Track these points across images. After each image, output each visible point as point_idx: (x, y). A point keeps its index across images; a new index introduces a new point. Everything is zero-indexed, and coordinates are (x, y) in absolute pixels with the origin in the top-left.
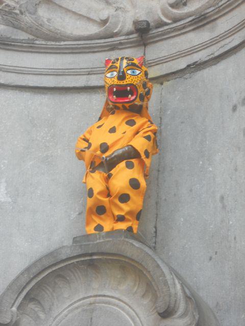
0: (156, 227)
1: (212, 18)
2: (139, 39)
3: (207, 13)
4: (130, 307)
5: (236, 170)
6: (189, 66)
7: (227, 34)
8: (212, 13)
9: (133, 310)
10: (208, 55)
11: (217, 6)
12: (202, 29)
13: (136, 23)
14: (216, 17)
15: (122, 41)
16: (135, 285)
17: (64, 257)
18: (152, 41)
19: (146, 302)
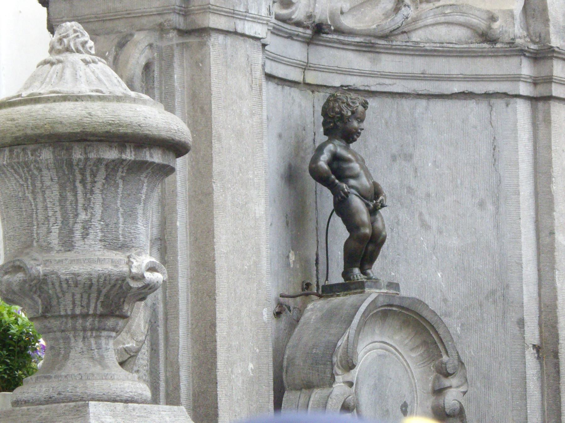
0: (317, 255)
1: (378, 50)
2: (311, 36)
3: (377, 44)
4: (403, 357)
5: (398, 223)
6: (342, 86)
7: (390, 75)
8: (382, 46)
9: (406, 361)
10: (363, 84)
11: (390, 43)
12: (362, 53)
13: (310, 17)
14: (382, 51)
15: (300, 34)
16: (407, 338)
17: (380, 305)
18: (317, 42)
19: (413, 355)
